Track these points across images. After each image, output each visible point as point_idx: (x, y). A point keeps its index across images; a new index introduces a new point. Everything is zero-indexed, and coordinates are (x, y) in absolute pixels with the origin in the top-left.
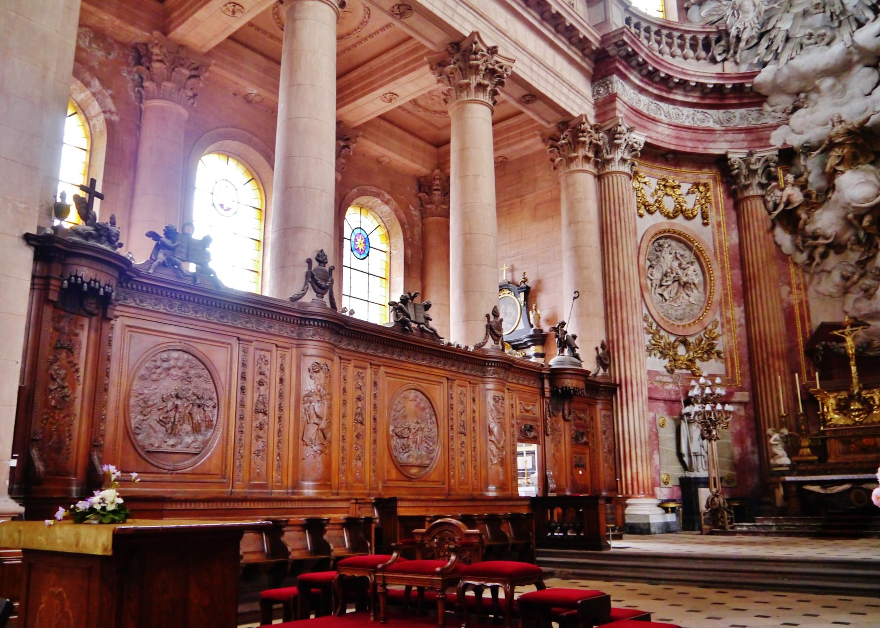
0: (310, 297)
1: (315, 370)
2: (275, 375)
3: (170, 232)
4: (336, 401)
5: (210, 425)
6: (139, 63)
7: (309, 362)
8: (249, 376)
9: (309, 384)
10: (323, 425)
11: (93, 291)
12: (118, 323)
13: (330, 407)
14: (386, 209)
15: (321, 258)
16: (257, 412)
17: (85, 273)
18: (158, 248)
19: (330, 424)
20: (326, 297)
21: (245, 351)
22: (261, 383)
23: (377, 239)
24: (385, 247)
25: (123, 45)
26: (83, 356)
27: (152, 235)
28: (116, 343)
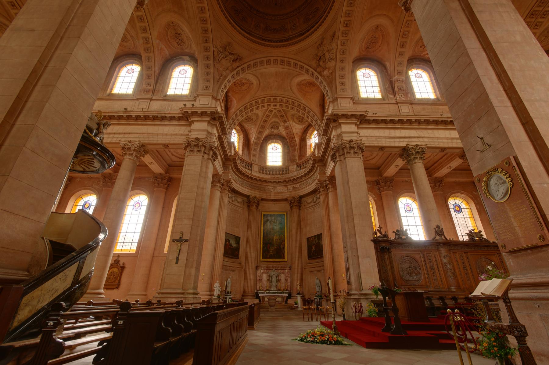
0: (438, 238)
1: (445, 257)
2: (434, 259)
3: (397, 231)
4: (455, 264)
5: (420, 273)
6: (377, 184)
7: (443, 255)
8: (426, 260)
9: (445, 261)
10: (452, 271)
11: (386, 248)
12: (392, 253)
13: (453, 266)
14: (463, 195)
15: (438, 227)
16: (431, 269)
17: (384, 245)
18: (396, 234)
19: (455, 271)
20: (443, 237)
21: (424, 254)
22: (430, 262)
23: (463, 205)
24: (468, 207)
25: (373, 182)
26: (387, 261)
27: (394, 232)
28: (393, 257)
